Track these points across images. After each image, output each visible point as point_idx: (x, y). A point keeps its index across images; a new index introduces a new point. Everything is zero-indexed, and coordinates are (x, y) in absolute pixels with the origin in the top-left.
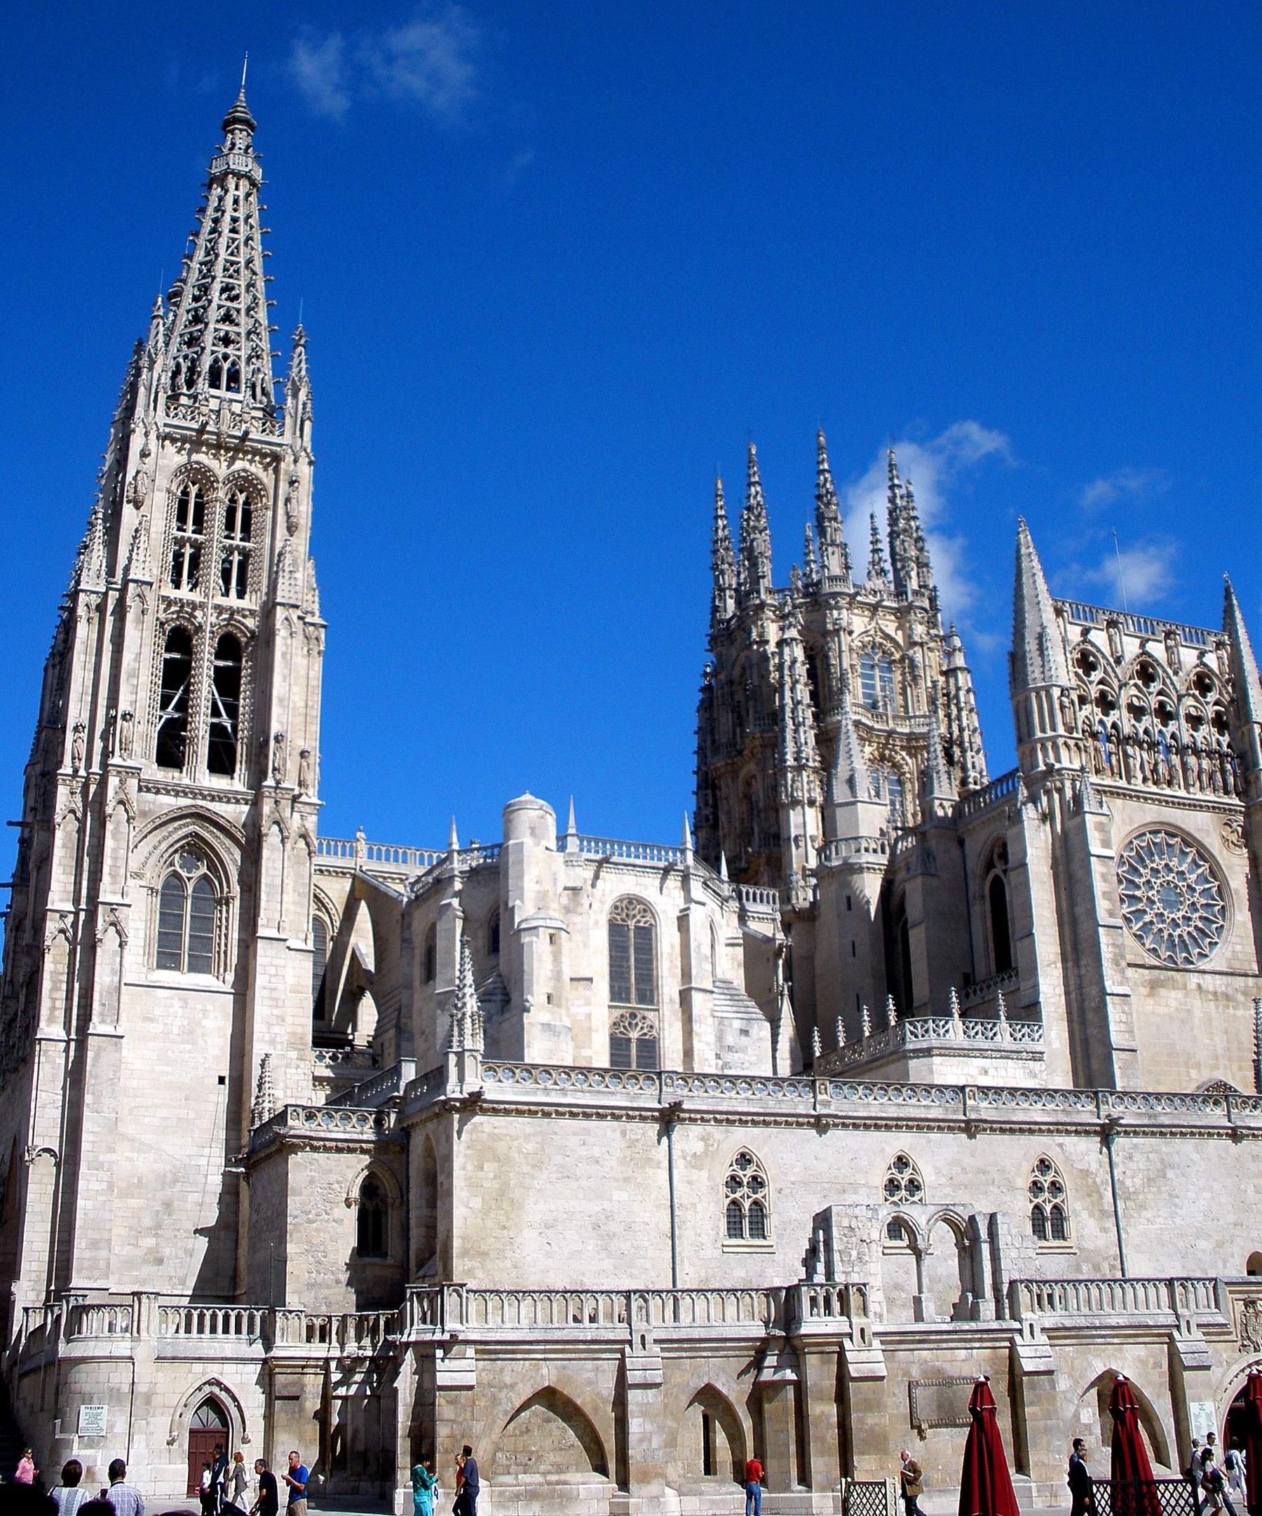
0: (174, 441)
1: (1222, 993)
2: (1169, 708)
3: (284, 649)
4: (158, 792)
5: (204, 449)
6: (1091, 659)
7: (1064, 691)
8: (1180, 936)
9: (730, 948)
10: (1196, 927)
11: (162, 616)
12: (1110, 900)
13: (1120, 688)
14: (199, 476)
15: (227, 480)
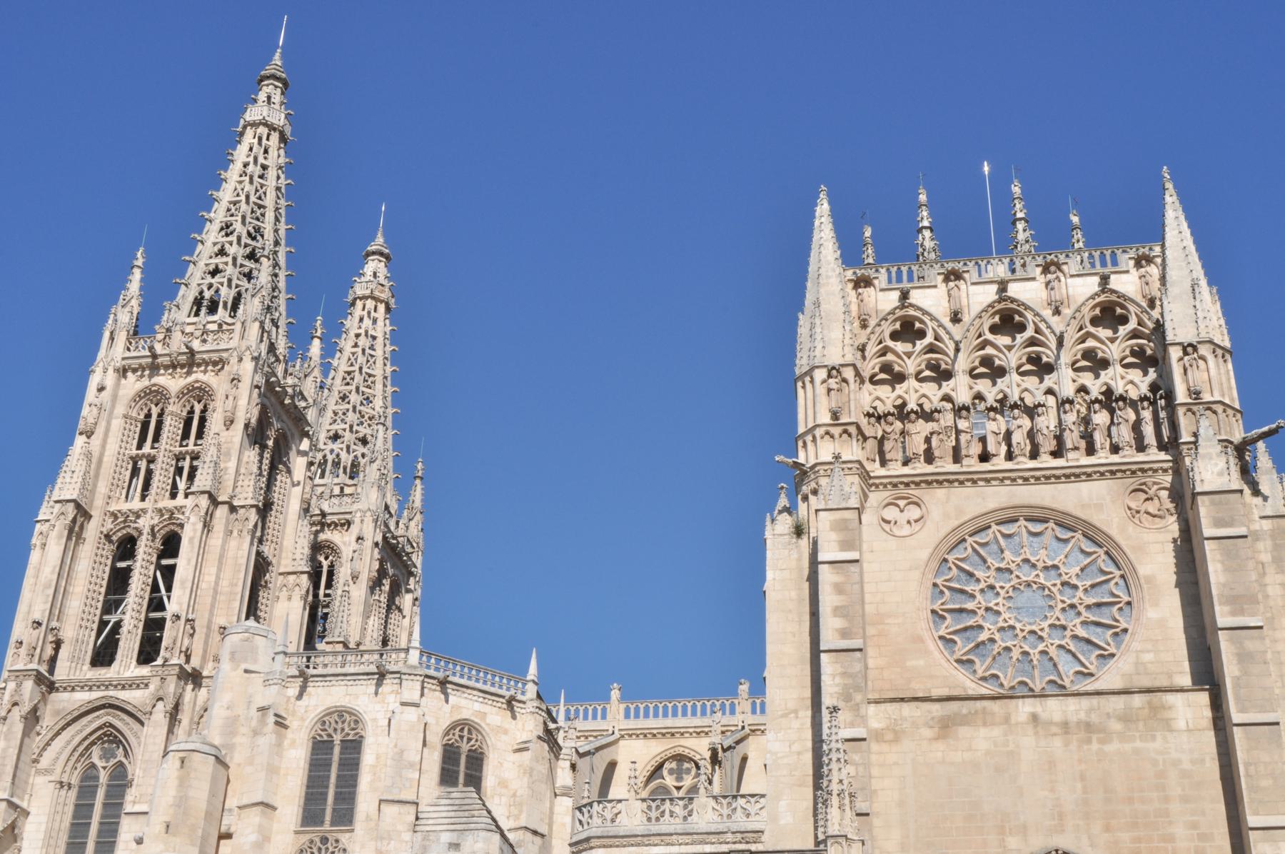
0: (134, 371)
1: (1079, 723)
2: (1045, 359)
3: (192, 534)
4: (73, 690)
5: (162, 371)
6: (917, 325)
7: (833, 371)
8: (1044, 653)
9: (517, 754)
10: (1075, 637)
11: (109, 525)
12: (845, 616)
13: (957, 350)
14: (156, 395)
15: (181, 394)
